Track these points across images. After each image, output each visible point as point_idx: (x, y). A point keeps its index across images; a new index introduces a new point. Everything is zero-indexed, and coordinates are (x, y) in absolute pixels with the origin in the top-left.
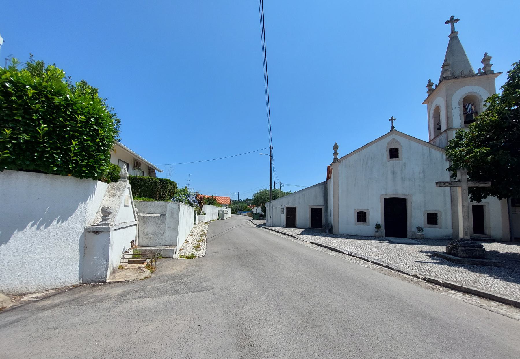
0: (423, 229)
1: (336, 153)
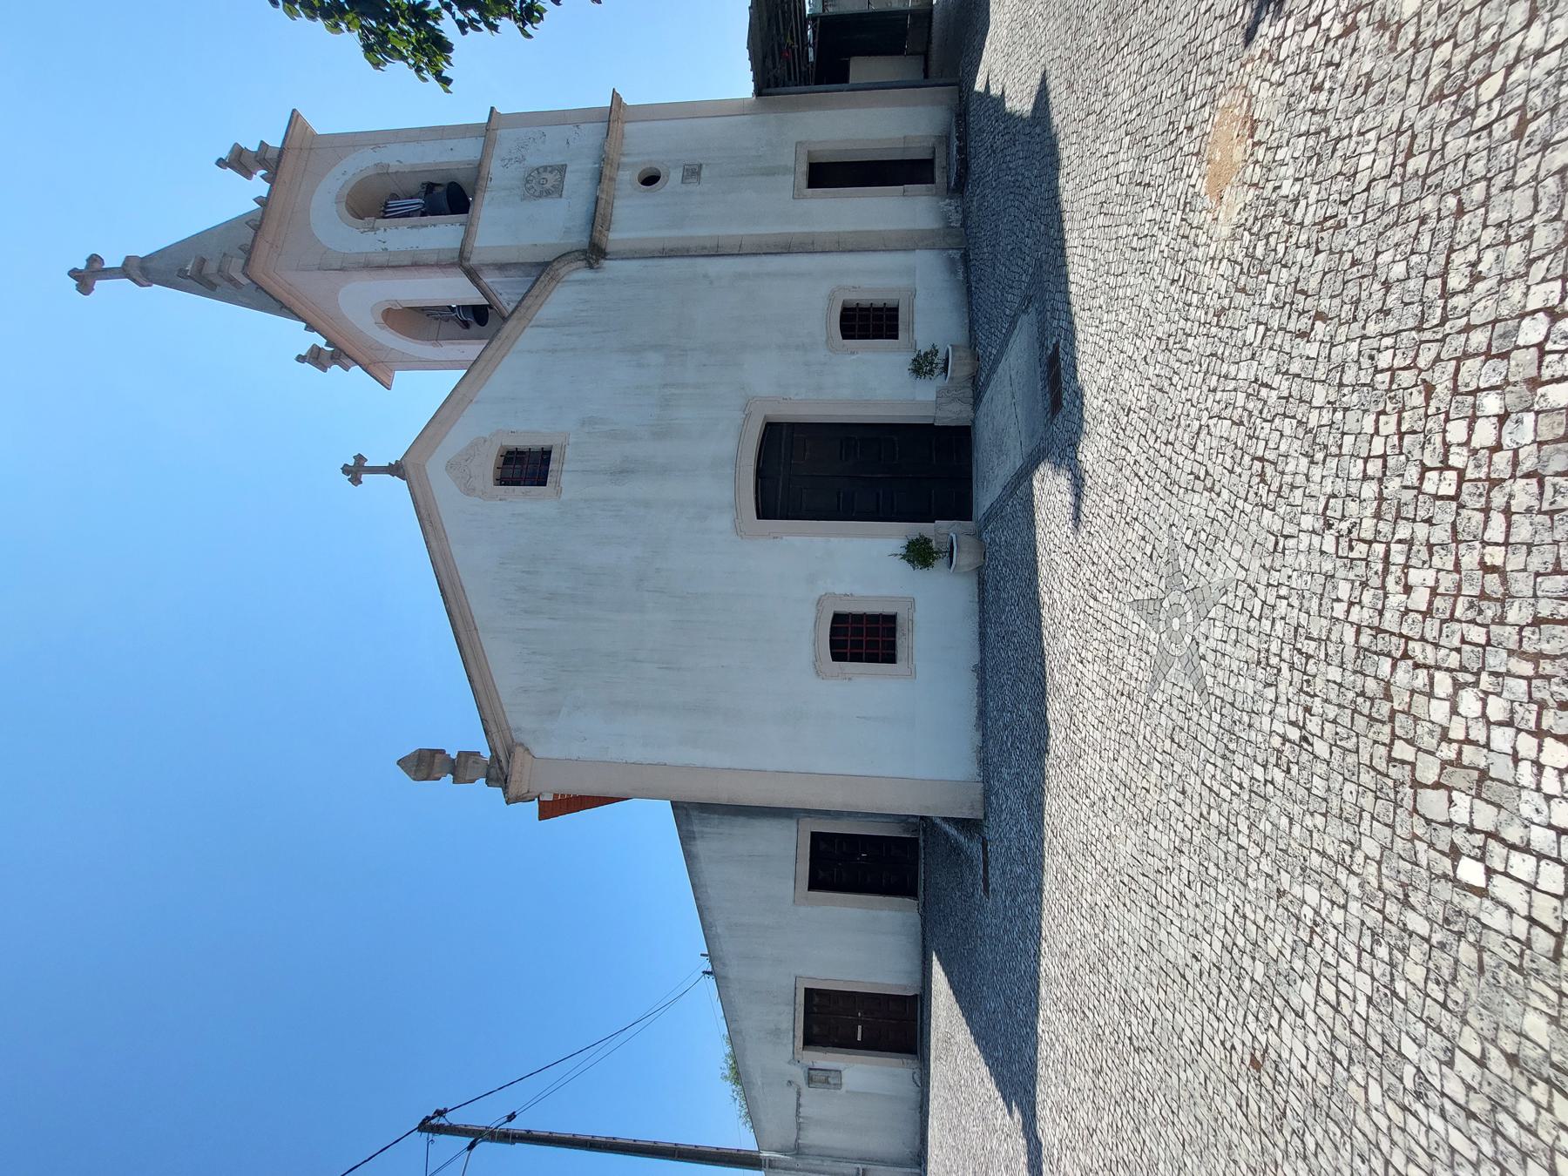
0: (924, 347)
1: (460, 767)
